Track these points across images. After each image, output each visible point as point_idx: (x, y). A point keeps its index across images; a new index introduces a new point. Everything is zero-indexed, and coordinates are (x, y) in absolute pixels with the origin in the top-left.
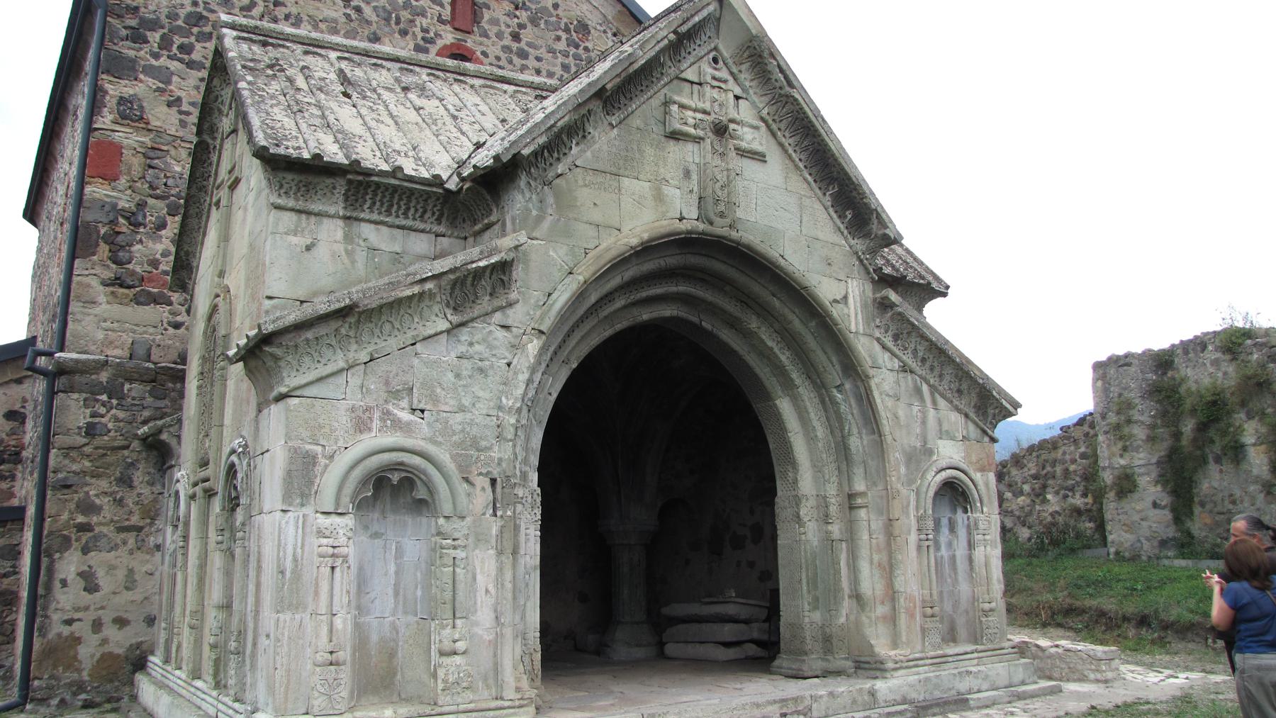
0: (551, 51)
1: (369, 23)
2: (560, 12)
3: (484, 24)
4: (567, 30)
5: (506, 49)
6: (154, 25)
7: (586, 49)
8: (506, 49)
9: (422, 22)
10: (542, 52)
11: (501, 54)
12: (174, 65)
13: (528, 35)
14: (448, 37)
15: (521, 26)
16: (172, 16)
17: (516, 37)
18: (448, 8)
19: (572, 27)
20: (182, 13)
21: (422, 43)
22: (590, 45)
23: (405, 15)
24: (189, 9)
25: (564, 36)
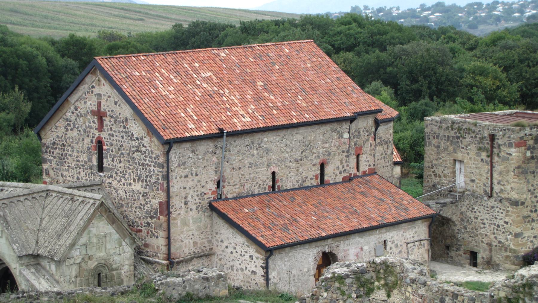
0: (119, 132)
1: (81, 135)
2: (121, 116)
3: (105, 127)
4: (123, 123)
5: (109, 135)
6: (48, 147)
7: (128, 128)
8: (109, 135)
9: (92, 131)
10: (118, 134)
11: (108, 137)
12: (52, 158)
13: (114, 128)
14: (97, 134)
15: (112, 125)
16: (50, 144)
17: (111, 129)
18: (97, 123)
19: (124, 121)
20: (52, 142)
21: (92, 138)
22: (128, 126)
23: (88, 129)
24: (53, 141)
25: (122, 124)
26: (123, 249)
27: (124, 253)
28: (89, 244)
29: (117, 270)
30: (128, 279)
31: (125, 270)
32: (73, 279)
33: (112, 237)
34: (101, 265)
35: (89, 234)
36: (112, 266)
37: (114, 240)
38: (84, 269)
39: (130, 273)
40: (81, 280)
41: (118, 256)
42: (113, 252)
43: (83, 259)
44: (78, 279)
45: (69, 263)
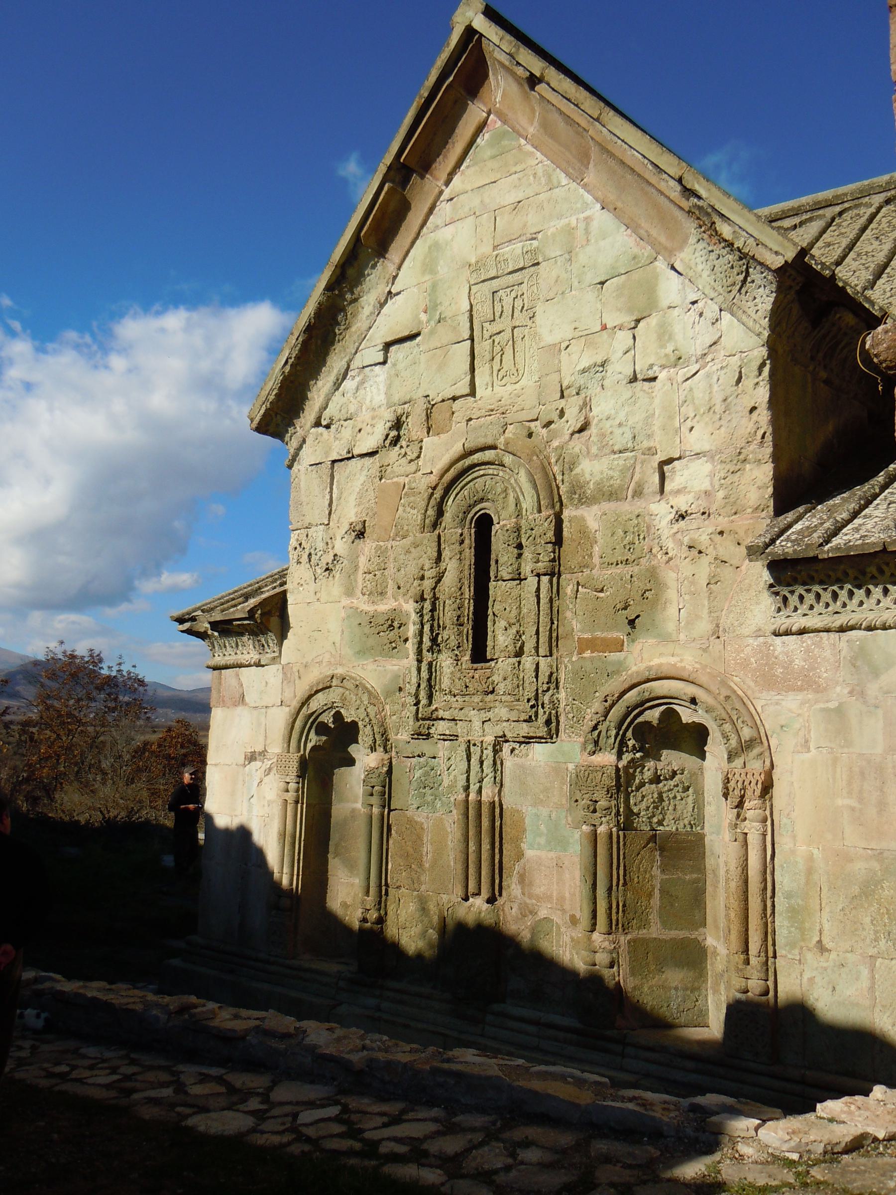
26: (664, 334)
27: (679, 360)
28: (432, 332)
29: (613, 495)
30: (704, 568)
31: (682, 503)
32: (341, 546)
33: (582, 258)
34: (489, 455)
35: (429, 267)
36: (572, 466)
37: (592, 277)
38: (397, 484)
39: (722, 522)
40: (381, 553)
41: (626, 392)
42: (585, 363)
43: (398, 424)
44: (368, 546)
45: (327, 454)
